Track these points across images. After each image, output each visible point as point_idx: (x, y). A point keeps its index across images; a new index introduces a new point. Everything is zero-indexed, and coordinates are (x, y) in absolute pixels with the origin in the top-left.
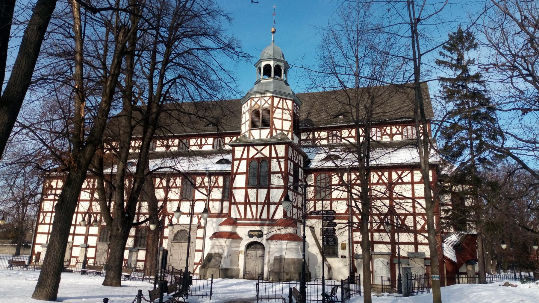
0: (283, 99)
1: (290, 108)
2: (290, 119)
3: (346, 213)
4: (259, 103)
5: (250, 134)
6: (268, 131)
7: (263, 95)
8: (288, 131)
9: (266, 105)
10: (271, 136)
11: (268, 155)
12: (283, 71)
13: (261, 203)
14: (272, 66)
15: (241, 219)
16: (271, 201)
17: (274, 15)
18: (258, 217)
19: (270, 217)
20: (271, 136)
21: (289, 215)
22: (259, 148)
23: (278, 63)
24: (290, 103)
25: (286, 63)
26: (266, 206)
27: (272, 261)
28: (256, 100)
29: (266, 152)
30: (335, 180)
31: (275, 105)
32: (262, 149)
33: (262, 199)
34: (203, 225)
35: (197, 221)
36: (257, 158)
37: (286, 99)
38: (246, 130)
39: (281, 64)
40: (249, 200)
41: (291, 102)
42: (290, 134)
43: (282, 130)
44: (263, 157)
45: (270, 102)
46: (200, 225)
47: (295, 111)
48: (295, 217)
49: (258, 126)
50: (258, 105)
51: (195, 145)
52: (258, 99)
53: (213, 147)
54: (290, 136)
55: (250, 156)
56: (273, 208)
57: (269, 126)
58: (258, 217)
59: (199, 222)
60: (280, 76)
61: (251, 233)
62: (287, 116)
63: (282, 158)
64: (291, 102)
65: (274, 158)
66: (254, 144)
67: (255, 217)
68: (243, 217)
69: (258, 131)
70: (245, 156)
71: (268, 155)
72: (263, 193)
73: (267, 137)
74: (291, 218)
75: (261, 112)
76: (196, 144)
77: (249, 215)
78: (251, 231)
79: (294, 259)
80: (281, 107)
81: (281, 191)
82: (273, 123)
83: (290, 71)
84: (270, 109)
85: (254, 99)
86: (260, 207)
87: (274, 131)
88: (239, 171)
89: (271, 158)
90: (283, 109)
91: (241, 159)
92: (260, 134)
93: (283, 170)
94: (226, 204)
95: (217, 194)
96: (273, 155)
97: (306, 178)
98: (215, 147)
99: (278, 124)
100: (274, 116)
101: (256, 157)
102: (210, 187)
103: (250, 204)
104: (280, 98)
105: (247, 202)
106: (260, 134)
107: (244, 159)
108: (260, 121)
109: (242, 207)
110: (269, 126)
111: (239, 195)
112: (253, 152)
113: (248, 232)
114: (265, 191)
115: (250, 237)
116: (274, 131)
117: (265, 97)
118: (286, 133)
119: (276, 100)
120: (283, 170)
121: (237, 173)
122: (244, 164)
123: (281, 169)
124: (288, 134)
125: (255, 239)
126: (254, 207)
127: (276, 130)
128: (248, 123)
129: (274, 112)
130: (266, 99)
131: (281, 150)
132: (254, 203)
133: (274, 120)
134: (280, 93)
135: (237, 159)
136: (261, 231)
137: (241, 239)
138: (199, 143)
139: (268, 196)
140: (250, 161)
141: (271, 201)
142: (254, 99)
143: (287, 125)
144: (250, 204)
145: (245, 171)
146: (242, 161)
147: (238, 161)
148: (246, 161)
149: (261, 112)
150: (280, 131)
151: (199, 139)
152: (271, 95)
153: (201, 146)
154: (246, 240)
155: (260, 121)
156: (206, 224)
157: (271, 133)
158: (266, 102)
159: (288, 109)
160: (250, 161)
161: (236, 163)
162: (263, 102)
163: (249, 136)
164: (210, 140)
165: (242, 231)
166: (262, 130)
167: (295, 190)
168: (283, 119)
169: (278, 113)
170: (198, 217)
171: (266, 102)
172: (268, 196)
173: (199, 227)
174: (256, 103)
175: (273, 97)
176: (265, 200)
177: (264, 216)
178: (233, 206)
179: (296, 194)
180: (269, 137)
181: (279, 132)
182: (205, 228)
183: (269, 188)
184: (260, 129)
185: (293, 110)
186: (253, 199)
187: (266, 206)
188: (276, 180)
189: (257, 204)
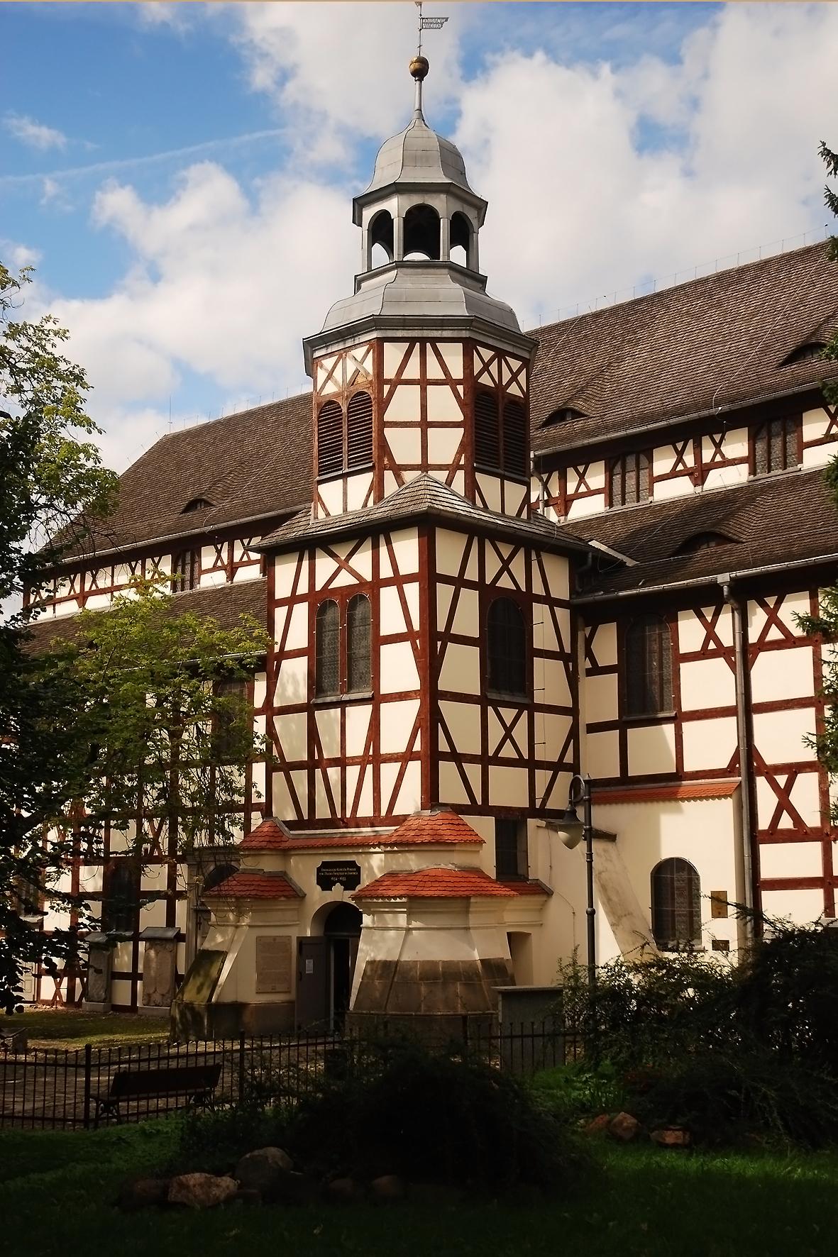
0: (423, 341)
1: (457, 372)
2: (460, 417)
3: (730, 771)
6: (368, 478)
7: (349, 343)
8: (453, 468)
10: (380, 497)
11: (368, 577)
13: (354, 761)
14: (394, 215)
16: (385, 749)
19: (383, 813)
20: (380, 497)
22: (342, 552)
23: (416, 200)
26: (370, 768)
29: (362, 562)
30: (690, 632)
31: (390, 373)
33: (356, 747)
39: (441, 205)
41: (459, 347)
42: (460, 475)
43: (425, 467)
49: (338, 465)
50: (336, 382)
55: (318, 587)
56: (389, 772)
57: (368, 458)
60: (434, 253)
61: (327, 872)
62: (445, 404)
63: (410, 578)
64: (459, 347)
70: (303, 589)
71: (368, 576)
73: (365, 505)
75: (344, 410)
77: (323, 812)
78: (325, 864)
79: (434, 964)
81: (414, 706)
82: (384, 448)
84: (370, 392)
87: (389, 476)
89: (378, 583)
90: (424, 382)
93: (416, 627)
96: (386, 572)
97: (588, 641)
99: (403, 446)
100: (388, 417)
105: (313, 764)
107: (302, 599)
108: (345, 448)
110: (368, 458)
112: (325, 566)
113: (319, 870)
114: (368, 709)
116: (389, 476)
118: (442, 476)
119: (394, 354)
120: (416, 627)
121: (284, 655)
123: (409, 622)
124: (449, 482)
125: (339, 894)
127: (398, 470)
129: (384, 404)
130: (359, 352)
131: (407, 551)
133: (387, 431)
134: (405, 322)
135: (282, 602)
136: (353, 864)
140: (320, 602)
141: (385, 749)
143: (446, 445)
145: (304, 644)
149: (344, 410)
152: (374, 335)
154: (318, 897)
155: (345, 448)
157: (378, 488)
159: (449, 381)
160: (320, 602)
161: (280, 613)
165: (304, 871)
168: (425, 425)
169: (404, 404)
175: (381, 341)
176: (367, 749)
177: (366, 810)
178: (278, 777)
180: (371, 503)
181: (409, 476)
183: (376, 700)
187: (370, 768)
188: (398, 668)
189: (342, 762)
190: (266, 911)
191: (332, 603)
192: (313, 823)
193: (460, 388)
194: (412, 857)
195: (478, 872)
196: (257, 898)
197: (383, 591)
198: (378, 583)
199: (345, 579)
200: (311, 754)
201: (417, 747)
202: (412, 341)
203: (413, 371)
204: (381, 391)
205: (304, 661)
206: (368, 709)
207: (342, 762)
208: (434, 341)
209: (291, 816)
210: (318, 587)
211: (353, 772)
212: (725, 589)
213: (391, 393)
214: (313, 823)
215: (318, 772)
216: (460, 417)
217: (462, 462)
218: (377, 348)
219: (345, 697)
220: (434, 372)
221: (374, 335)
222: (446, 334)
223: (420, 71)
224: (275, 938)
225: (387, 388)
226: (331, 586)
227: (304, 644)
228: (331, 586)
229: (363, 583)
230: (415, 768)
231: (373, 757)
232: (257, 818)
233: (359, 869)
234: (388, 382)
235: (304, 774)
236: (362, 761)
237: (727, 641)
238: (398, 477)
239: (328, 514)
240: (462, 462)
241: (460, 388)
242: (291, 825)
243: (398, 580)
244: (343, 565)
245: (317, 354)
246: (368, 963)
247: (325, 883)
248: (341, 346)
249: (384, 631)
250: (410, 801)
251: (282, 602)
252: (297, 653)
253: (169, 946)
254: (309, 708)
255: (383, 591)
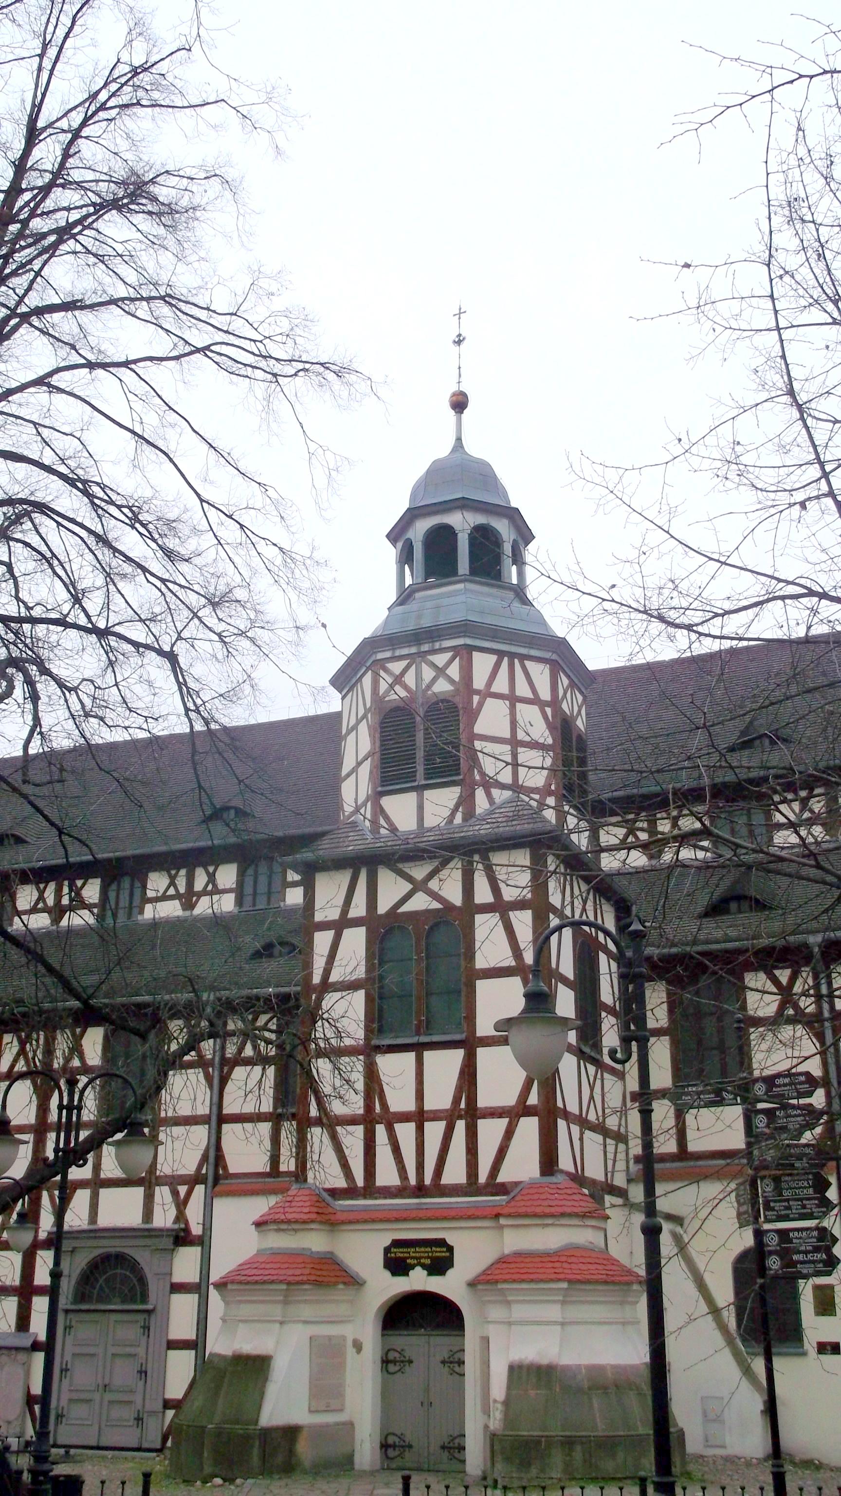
0: (512, 656)
1: (545, 694)
2: (550, 741)
4: (410, 679)
5: (379, 811)
7: (425, 647)
8: (545, 791)
9: (442, 687)
10: (469, 814)
12: (507, 548)
13: (435, 1116)
15: (351, 1192)
17: (459, 342)
18: (428, 1181)
19: (482, 1178)
20: (469, 814)
21: (565, 1162)
22: (419, 872)
23: (480, 519)
24: (541, 674)
25: (514, 516)
26: (460, 1126)
27: (498, 1389)
28: (396, 667)
31: (479, 683)
32: (431, 876)
34: (196, 1230)
35: (173, 1212)
36: (413, 916)
37: (523, 658)
38: (362, 798)
40: (384, 1105)
42: (551, 801)
44: (436, 905)
45: (454, 671)
46: (187, 1230)
47: (565, 706)
48: (594, 1171)
49: (412, 777)
50: (406, 687)
51: (164, 898)
52: (403, 664)
53: (239, 902)
54: (550, 815)
55: (383, 908)
56: (490, 1132)
57: (455, 769)
58: (428, 1181)
59: (181, 1216)
61: (399, 1252)
62: (535, 724)
63: (520, 905)
65: (486, 909)
66: (397, 856)
67: (413, 1181)
68: (360, 1182)
69: (412, 797)
70: (358, 909)
72: (444, 1066)
74: (578, 1178)
76: (172, 891)
77: (387, 1174)
78: (397, 1243)
80: (505, 690)
82: (474, 762)
83: (531, 553)
84: (457, 700)
85: (390, 666)
86: (434, 1131)
87: (480, 793)
88: (334, 978)
90: (513, 699)
91: (340, 925)
92: (420, 808)
93: (529, 958)
94: (288, 1129)
95: (251, 1088)
96: (483, 894)
98: (248, 900)
99: (492, 762)
101: (404, 909)
102: (224, 1061)
103: (391, 1120)
104: (501, 654)
106: (420, 808)
107: (357, 922)
108: (420, 754)
109: (353, 1139)
111: (339, 1085)
112: (391, 890)
113: (387, 1250)
114: (457, 1056)
115: (395, 1273)
117: (434, 652)
119: (482, 664)
121: (326, 986)
122: (355, 941)
125: (419, 1280)
126: (406, 1132)
128: (366, 769)
129: (473, 715)
130: (440, 659)
132: (405, 1117)
134: (495, 633)
135: (324, 926)
137: (353, 1282)
138: (182, 890)
139: (468, 1076)
140: (384, 930)
141: (483, 1101)
142: (390, 666)
143: (536, 768)
144: (391, 1120)
146: (347, 933)
147: (330, 934)
148: (363, 930)
150: (507, 794)
151: (183, 872)
152: (460, 641)
153: (188, 899)
155: (420, 754)
156: (208, 1225)
157: (466, 802)
158: (441, 671)
159: (535, 701)
160: (384, 930)
161: (322, 941)
162: (428, 674)
163: (374, 822)
164: (227, 875)
166: (427, 794)
167: (588, 1049)
168: (514, 743)
169: (492, 719)
170: (175, 1193)
171: (441, 671)
172: (468, 1076)
173: (181, 1237)
174: (398, 680)
175: (471, 649)
176: (456, 1101)
177: (455, 1172)
179: (592, 1069)
180: (458, 819)
182: (203, 1241)
183: (470, 1045)
184: (420, 789)
185: (555, 702)
186: (400, 1098)
187: (460, 1126)
189: (420, 1117)
190: (317, 1302)
191: (402, 929)
192: (370, 1189)
193: (549, 710)
194: (550, 1231)
195: (603, 1258)
196: (318, 1284)
197: (479, 919)
198: (470, 908)
199: (420, 902)
200: (369, 1107)
201: (533, 1099)
202: (501, 654)
203: (501, 685)
204: (470, 701)
205: (360, 996)
206: (457, 1056)
207: (420, 1117)
208: (523, 658)
209: (341, 1183)
210: (383, 908)
211: (434, 1131)
212: (816, 949)
213: (481, 704)
214: (370, 1189)
215: (381, 1130)
216: (550, 741)
217: (553, 787)
218: (465, 654)
219: (424, 1039)
220: (523, 689)
221: (460, 641)
222: (533, 652)
223: (459, 404)
224: (330, 1338)
225: (476, 699)
226: (404, 909)
227: (361, 973)
228: (401, 910)
229: (449, 907)
230: (529, 1127)
231: (467, 1109)
232: (163, 1194)
233: (450, 1249)
234: (478, 692)
235: (359, 1130)
236: (450, 1117)
237: (808, 1004)
238: (489, 795)
239: (393, 829)
240: (553, 787)
241: (549, 710)
242: (334, 1193)
243: (501, 908)
244: (418, 886)
245: (380, 656)
246: (516, 1371)
247: (397, 1265)
248: (413, 650)
249: (481, 962)
250: (523, 1164)
251: (324, 926)
252: (352, 986)
253: (22, 1357)
254: (370, 1050)
255: (479, 919)
